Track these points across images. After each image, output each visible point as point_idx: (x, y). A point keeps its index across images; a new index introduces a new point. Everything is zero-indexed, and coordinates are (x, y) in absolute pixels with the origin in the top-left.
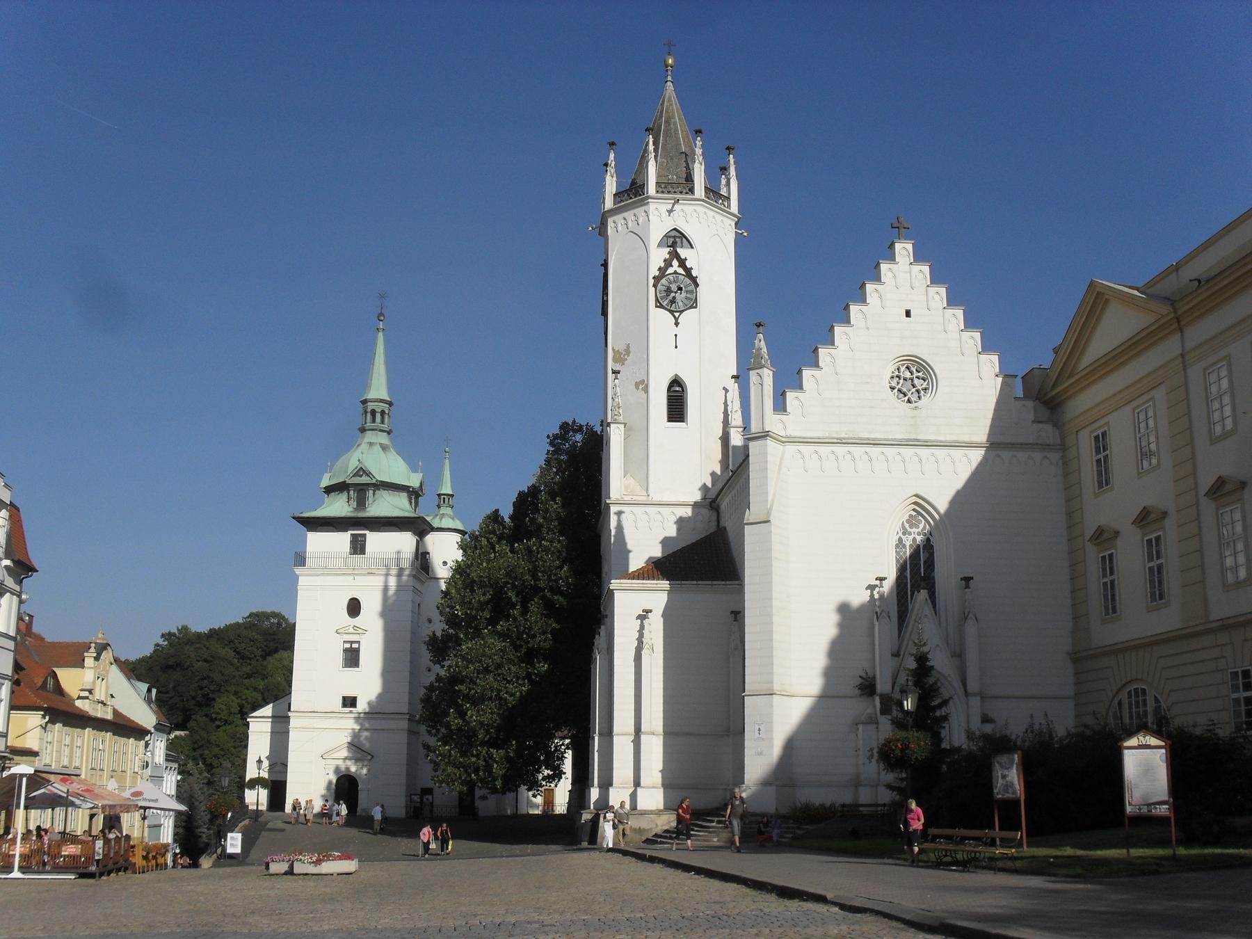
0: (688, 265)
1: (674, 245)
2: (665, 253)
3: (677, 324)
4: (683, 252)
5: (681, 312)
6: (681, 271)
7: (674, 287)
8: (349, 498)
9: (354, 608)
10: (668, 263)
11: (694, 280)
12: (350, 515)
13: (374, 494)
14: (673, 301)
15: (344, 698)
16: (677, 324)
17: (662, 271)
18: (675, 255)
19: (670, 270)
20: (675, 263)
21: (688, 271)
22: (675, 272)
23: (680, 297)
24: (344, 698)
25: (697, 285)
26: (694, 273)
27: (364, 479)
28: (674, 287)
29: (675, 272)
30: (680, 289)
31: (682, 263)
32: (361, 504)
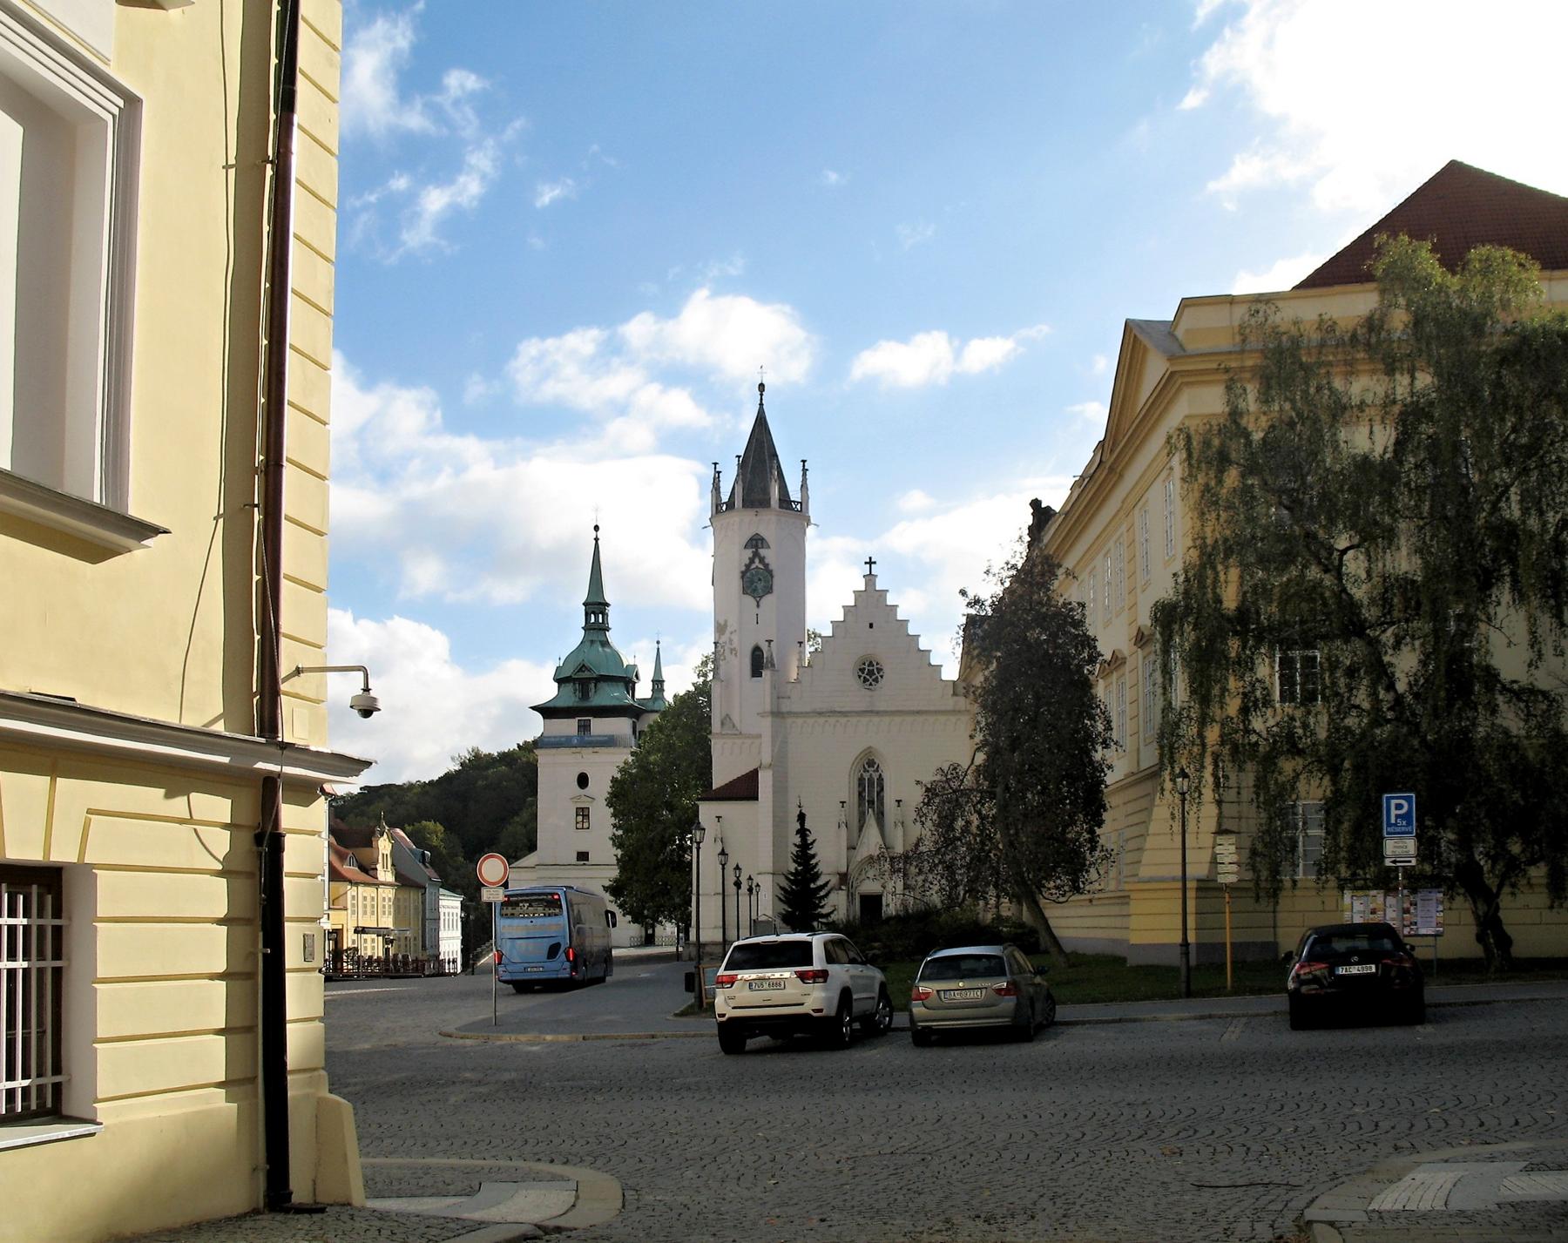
0: (766, 561)
1: (756, 547)
2: (749, 553)
3: (758, 606)
4: (762, 552)
5: (761, 597)
6: (761, 566)
7: (756, 579)
8: (575, 690)
9: (583, 781)
10: (752, 561)
11: (770, 573)
12: (576, 705)
13: (595, 686)
14: (755, 590)
15: (578, 853)
16: (758, 606)
17: (748, 566)
18: (756, 554)
19: (753, 566)
20: (757, 561)
21: (766, 566)
22: (757, 567)
23: (760, 585)
24: (578, 853)
25: (772, 577)
26: (770, 568)
27: (586, 675)
28: (756, 579)
29: (757, 567)
30: (760, 580)
31: (762, 560)
32: (585, 695)
